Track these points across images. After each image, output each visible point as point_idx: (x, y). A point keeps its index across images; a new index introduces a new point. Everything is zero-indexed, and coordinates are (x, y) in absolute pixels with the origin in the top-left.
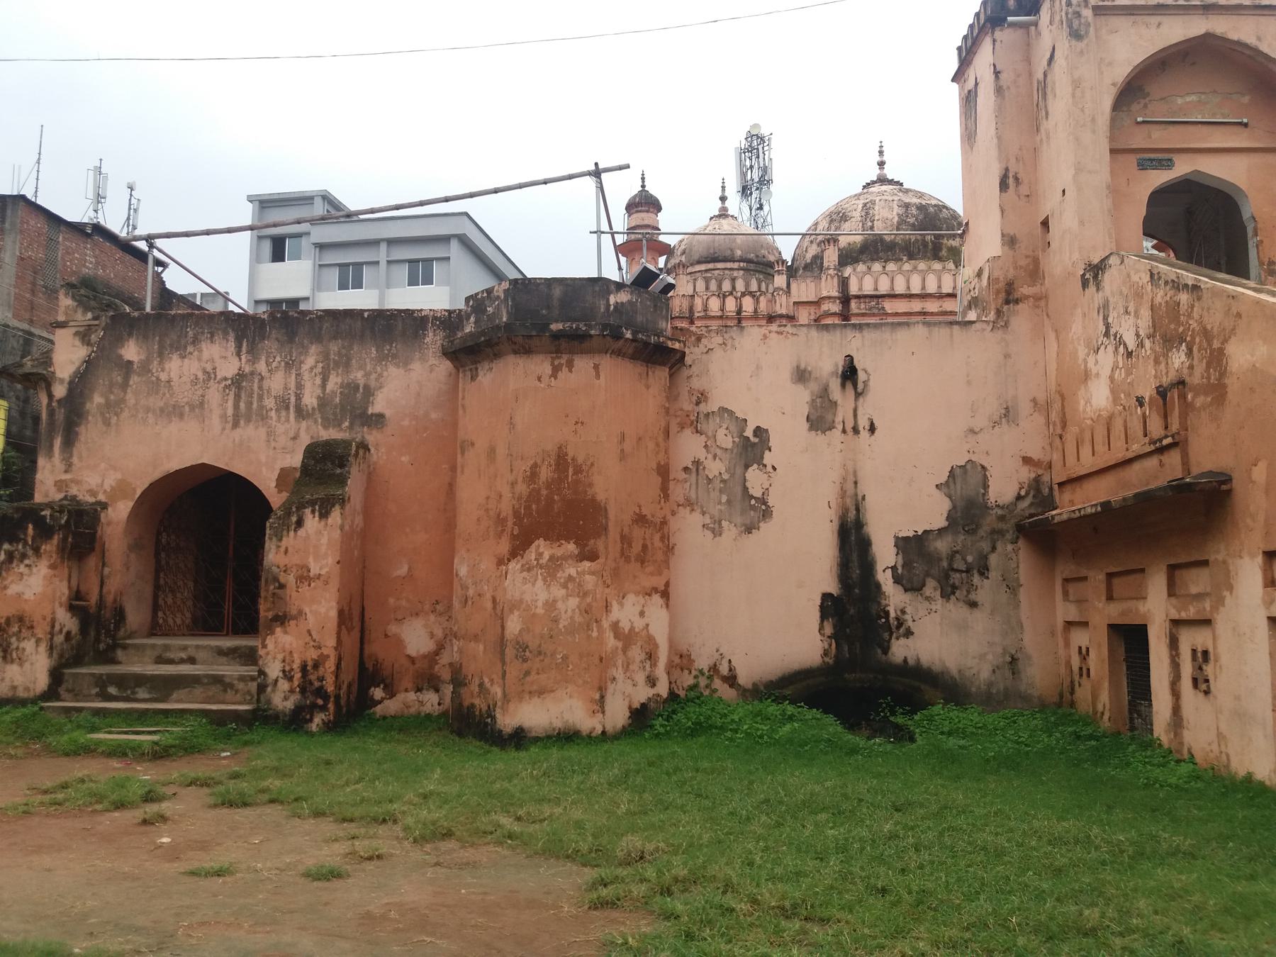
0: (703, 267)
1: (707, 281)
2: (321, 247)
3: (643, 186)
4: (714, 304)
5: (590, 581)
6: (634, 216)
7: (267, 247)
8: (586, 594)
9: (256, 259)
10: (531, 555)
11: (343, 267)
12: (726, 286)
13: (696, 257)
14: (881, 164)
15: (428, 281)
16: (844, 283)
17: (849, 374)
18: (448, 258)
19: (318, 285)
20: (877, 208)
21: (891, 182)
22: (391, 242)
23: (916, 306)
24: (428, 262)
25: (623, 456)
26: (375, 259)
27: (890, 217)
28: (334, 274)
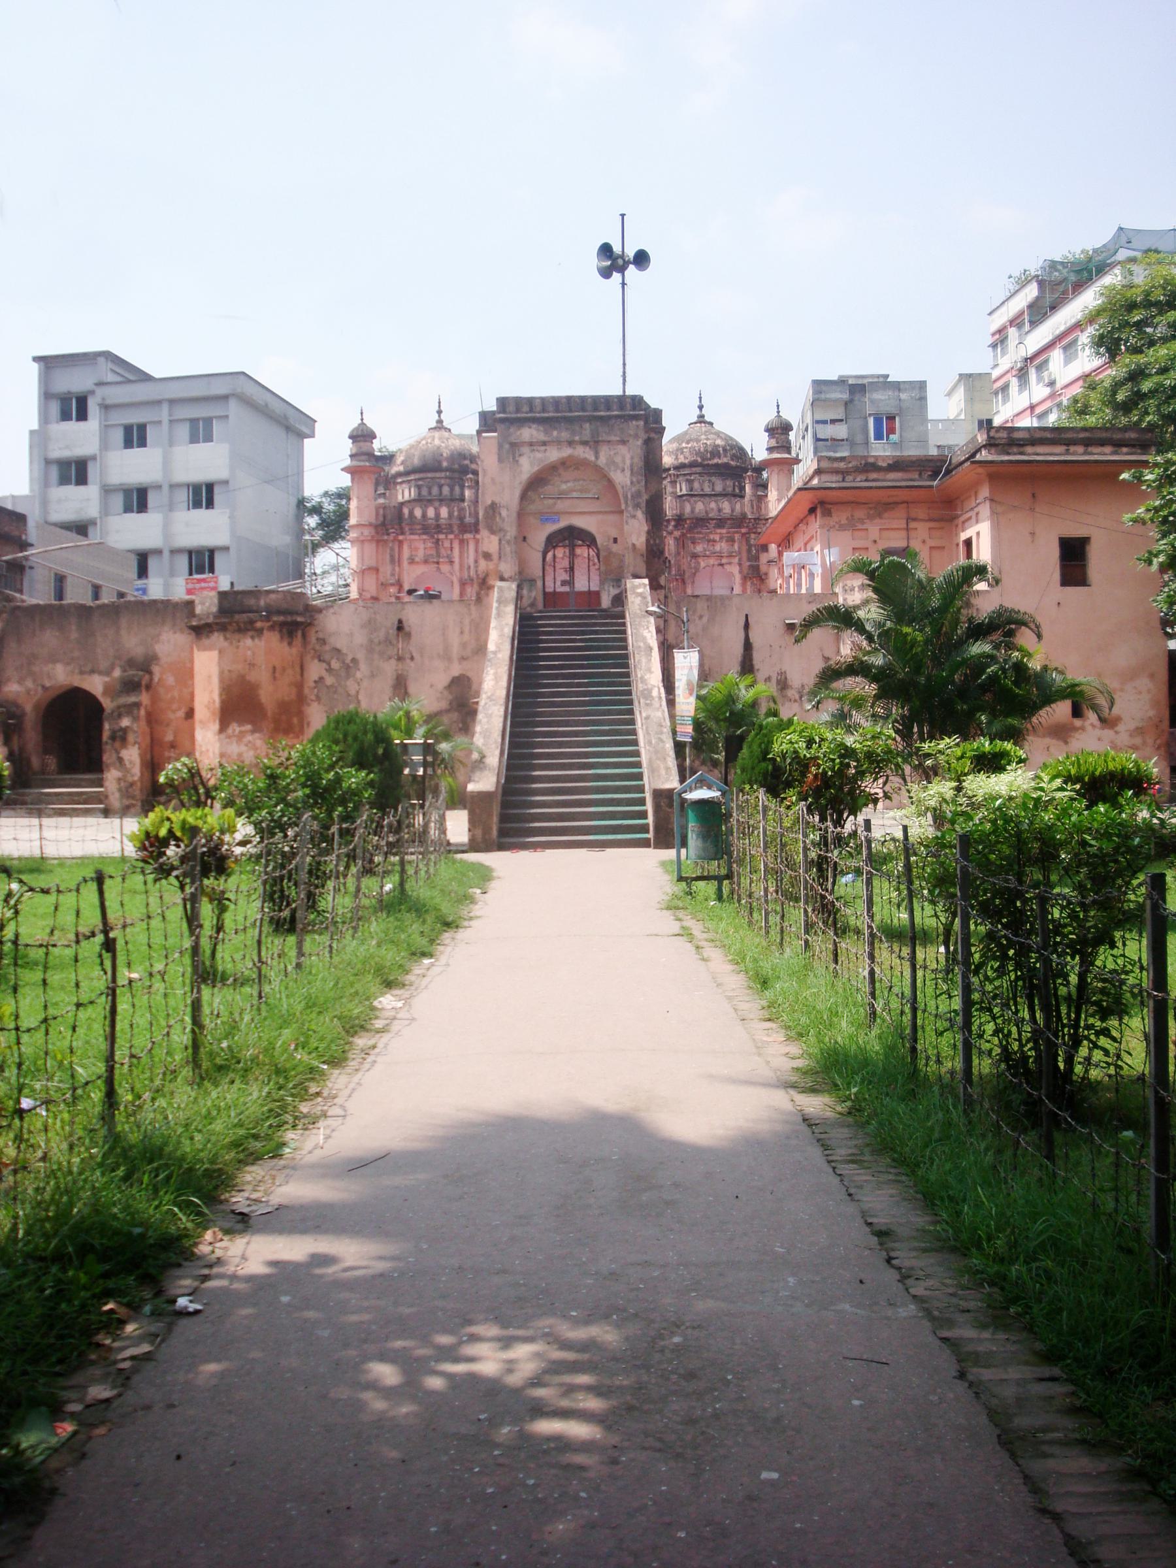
0: (417, 476)
1: (419, 487)
2: (106, 407)
4: (418, 513)
5: (259, 743)
8: (257, 749)
9: (44, 419)
10: (230, 731)
13: (410, 468)
15: (209, 438)
17: (400, 627)
18: (227, 417)
19: (105, 445)
22: (172, 402)
24: (208, 421)
25: (275, 678)
26: (156, 419)
28: (118, 436)
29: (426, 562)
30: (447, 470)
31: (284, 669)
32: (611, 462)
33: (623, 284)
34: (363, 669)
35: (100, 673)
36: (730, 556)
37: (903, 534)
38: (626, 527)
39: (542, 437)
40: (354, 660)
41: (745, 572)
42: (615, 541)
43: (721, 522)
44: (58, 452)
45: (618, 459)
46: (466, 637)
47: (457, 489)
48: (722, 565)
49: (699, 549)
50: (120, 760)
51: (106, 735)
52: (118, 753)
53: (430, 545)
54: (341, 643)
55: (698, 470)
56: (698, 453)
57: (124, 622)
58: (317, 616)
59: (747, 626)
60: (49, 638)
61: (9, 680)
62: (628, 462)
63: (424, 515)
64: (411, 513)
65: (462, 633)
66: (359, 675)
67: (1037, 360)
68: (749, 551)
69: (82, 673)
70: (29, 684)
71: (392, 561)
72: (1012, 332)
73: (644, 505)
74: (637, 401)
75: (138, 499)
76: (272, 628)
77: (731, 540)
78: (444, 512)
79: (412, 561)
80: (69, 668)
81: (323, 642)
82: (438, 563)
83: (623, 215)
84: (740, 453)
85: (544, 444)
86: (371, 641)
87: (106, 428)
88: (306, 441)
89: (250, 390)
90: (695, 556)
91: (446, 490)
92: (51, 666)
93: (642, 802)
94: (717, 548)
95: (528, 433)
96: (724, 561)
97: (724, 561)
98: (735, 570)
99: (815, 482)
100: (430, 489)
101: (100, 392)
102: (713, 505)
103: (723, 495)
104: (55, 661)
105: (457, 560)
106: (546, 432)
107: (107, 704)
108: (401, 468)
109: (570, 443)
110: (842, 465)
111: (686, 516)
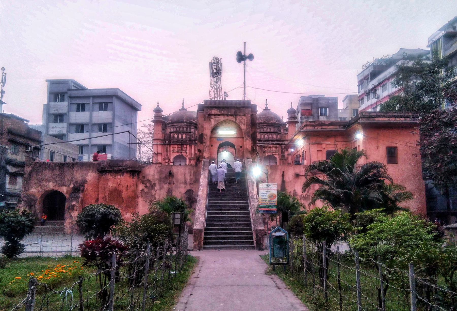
0: (176, 124)
1: (176, 128)
2: (71, 97)
4: (176, 136)
7: (53, 96)
9: (49, 100)
11: (78, 105)
15: (106, 109)
18: (112, 103)
19: (70, 110)
22: (94, 97)
24: (106, 104)
28: (75, 107)
29: (178, 152)
31: (131, 186)
32: (240, 122)
33: (245, 65)
34: (157, 187)
35: (66, 186)
37: (333, 146)
38: (245, 143)
39: (218, 113)
40: (155, 184)
41: (280, 157)
42: (241, 147)
43: (273, 141)
44: (52, 111)
45: (243, 121)
46: (192, 177)
47: (189, 129)
48: (273, 155)
50: (71, 216)
51: (66, 207)
52: (70, 213)
54: (150, 178)
55: (266, 124)
56: (266, 119)
57: (75, 168)
58: (143, 169)
59: (283, 175)
60: (48, 174)
61: (32, 187)
62: (246, 122)
64: (174, 136)
65: (191, 175)
66: (156, 188)
67: (374, 90)
68: (282, 150)
69: (59, 186)
70: (39, 189)
71: (167, 151)
72: (365, 81)
73: (250, 136)
74: (249, 102)
75: (81, 128)
76: (128, 172)
77: (276, 147)
79: (173, 152)
80: (54, 184)
81: (144, 177)
82: (182, 152)
83: (245, 43)
84: (279, 120)
85: (219, 115)
86: (160, 177)
87: (71, 104)
88: (138, 112)
89: (120, 94)
90: (264, 152)
91: (185, 129)
92: (48, 183)
93: (252, 234)
95: (214, 112)
96: (274, 154)
97: (274, 154)
99: (305, 129)
100: (180, 129)
101: (69, 92)
102: (270, 136)
103: (274, 133)
104: (49, 182)
106: (219, 112)
107: (67, 196)
108: (171, 122)
109: (227, 115)
110: (314, 124)
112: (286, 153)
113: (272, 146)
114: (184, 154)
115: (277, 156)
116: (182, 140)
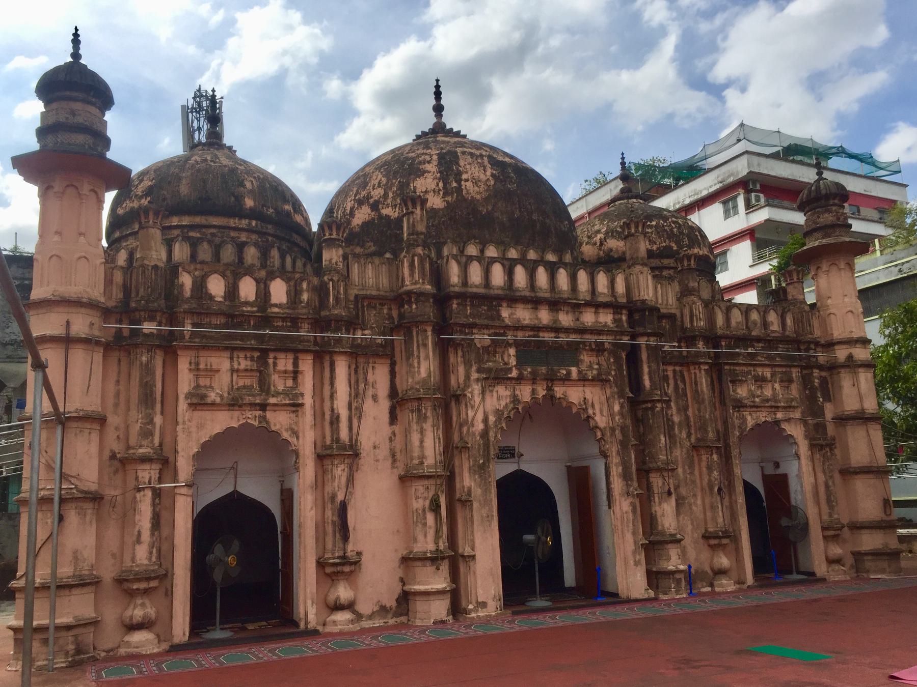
0: (186, 221)
1: (194, 244)
3: (76, 55)
4: (216, 286)
6: (55, 105)
12: (228, 254)
14: (438, 109)
16: (438, 276)
20: (462, 163)
21: (458, 134)
23: (544, 316)
27: (482, 177)
29: (234, 403)
30: (253, 214)
36: (788, 408)
43: (770, 342)
47: (275, 253)
48: (777, 423)
49: (742, 392)
53: (244, 364)
63: (232, 292)
64: (200, 286)
71: (147, 399)
77: (787, 381)
78: (279, 291)
79: (199, 402)
82: (263, 407)
90: (739, 405)
94: (768, 392)
96: (780, 415)
97: (780, 415)
98: (796, 431)
105: (308, 400)
111: (720, 332)
112: (829, 411)
113: (767, 373)
114: (279, 420)
115: (796, 431)
116: (265, 320)
